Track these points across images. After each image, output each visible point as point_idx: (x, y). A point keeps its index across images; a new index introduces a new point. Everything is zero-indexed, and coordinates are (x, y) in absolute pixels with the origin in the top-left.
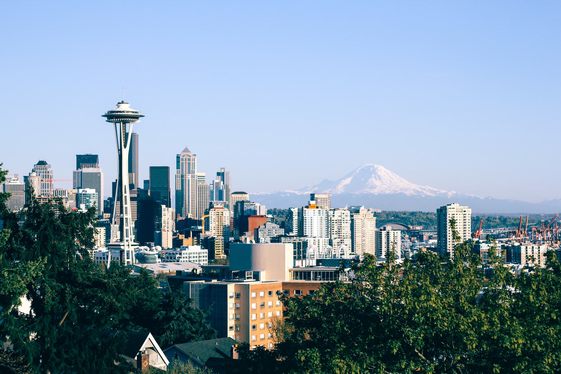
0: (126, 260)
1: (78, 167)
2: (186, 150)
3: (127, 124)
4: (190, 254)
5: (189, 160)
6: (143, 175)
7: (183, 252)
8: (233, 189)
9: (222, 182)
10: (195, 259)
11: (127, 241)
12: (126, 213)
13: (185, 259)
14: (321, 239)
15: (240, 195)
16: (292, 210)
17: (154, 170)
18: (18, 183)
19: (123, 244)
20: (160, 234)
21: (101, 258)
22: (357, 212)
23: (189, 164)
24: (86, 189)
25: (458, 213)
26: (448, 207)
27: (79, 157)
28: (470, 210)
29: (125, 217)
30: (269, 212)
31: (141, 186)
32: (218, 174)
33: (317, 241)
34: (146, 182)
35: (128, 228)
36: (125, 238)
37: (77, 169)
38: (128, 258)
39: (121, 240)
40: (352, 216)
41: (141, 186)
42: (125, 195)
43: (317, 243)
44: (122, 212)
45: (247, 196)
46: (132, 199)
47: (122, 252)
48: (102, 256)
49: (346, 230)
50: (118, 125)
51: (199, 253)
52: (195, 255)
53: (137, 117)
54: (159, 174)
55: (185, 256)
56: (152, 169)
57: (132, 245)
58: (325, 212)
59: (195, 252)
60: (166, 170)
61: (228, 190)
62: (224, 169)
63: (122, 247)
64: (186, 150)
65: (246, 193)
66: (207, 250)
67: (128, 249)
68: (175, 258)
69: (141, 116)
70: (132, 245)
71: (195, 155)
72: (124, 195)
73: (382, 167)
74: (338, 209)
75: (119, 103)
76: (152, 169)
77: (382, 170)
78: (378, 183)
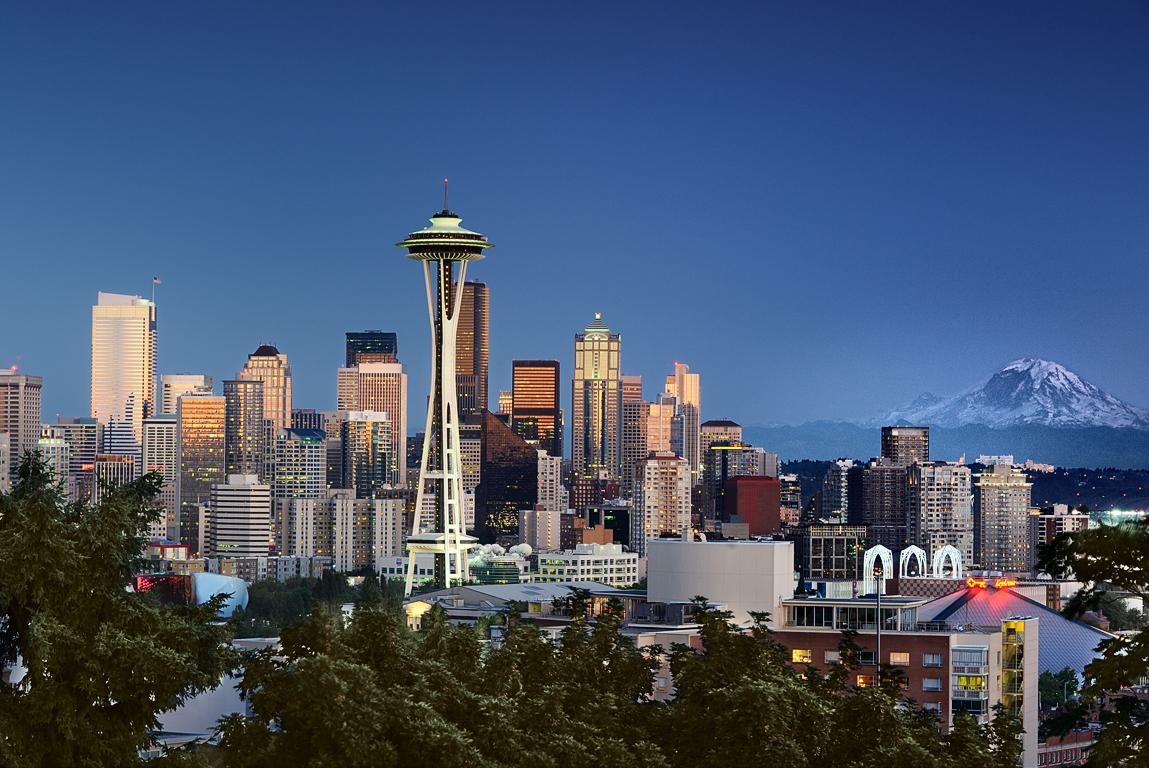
0: (449, 577)
4: (597, 562)
7: (582, 558)
11: (451, 531)
13: (586, 576)
15: (721, 429)
16: (840, 463)
19: (442, 538)
21: (392, 571)
24: (366, 412)
27: (350, 336)
29: (446, 476)
30: (787, 468)
36: (447, 526)
38: (453, 572)
39: (440, 529)
40: (975, 480)
42: (449, 426)
44: (440, 468)
45: (739, 430)
46: (464, 434)
47: (440, 557)
48: (396, 567)
49: (962, 512)
51: (621, 561)
52: (609, 566)
55: (586, 567)
57: (462, 542)
59: (609, 558)
63: (440, 548)
65: (736, 425)
67: (453, 551)
70: (462, 542)
72: (445, 426)
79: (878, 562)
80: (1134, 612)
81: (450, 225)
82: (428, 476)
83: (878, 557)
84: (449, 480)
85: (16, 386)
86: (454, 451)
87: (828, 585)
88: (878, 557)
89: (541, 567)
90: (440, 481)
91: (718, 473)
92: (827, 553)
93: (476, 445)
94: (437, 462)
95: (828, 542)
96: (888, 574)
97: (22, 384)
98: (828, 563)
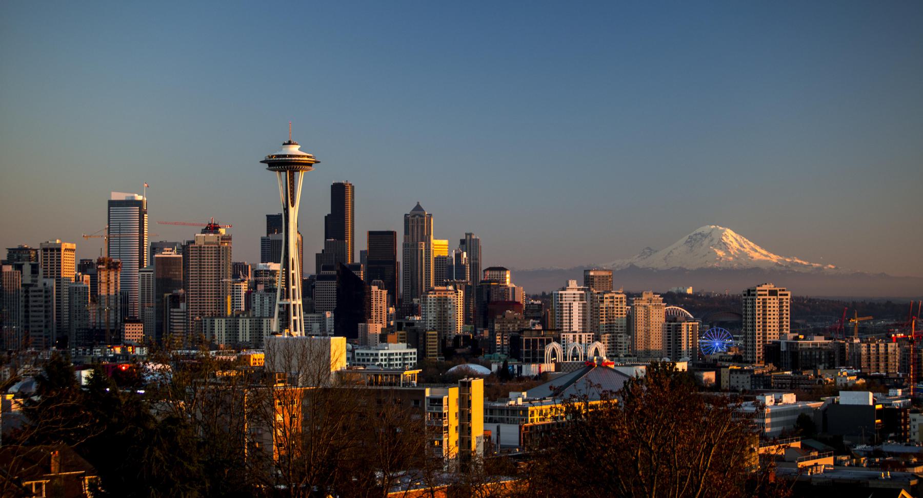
1: (270, 230)
2: (418, 207)
3: (296, 173)
5: (423, 221)
6: (359, 244)
7: (381, 352)
8: (484, 265)
9: (465, 254)
10: (398, 362)
12: (294, 298)
14: (583, 335)
15: (497, 273)
17: (374, 236)
18: (174, 255)
20: (366, 329)
22: (639, 295)
23: (423, 227)
24: (269, 264)
25: (772, 297)
26: (758, 288)
27: (268, 216)
28: (789, 293)
31: (357, 260)
32: (463, 242)
33: (577, 337)
34: (361, 252)
35: (297, 318)
37: (268, 234)
41: (357, 260)
43: (577, 339)
44: (288, 297)
50: (283, 174)
51: (405, 354)
52: (398, 357)
53: (310, 165)
54: (381, 240)
55: (384, 357)
56: (371, 234)
58: (589, 296)
59: (398, 351)
60: (390, 236)
61: (475, 267)
62: (471, 234)
64: (418, 207)
66: (415, 350)
68: (368, 360)
69: (316, 162)
71: (430, 215)
72: (291, 272)
73: (728, 230)
74: (610, 292)
75: (284, 144)
76: (371, 234)
77: (730, 236)
78: (720, 253)
79: (554, 354)
80: (708, 380)
81: (294, 150)
82: (281, 303)
83: (554, 350)
84: (294, 305)
85: (59, 250)
86: (296, 287)
87: (524, 367)
88: (554, 350)
89: (356, 357)
90: (288, 306)
91: (485, 299)
92: (535, 346)
93: (333, 285)
94: (286, 294)
95: (535, 341)
96: (560, 359)
97: (63, 249)
98: (535, 354)
